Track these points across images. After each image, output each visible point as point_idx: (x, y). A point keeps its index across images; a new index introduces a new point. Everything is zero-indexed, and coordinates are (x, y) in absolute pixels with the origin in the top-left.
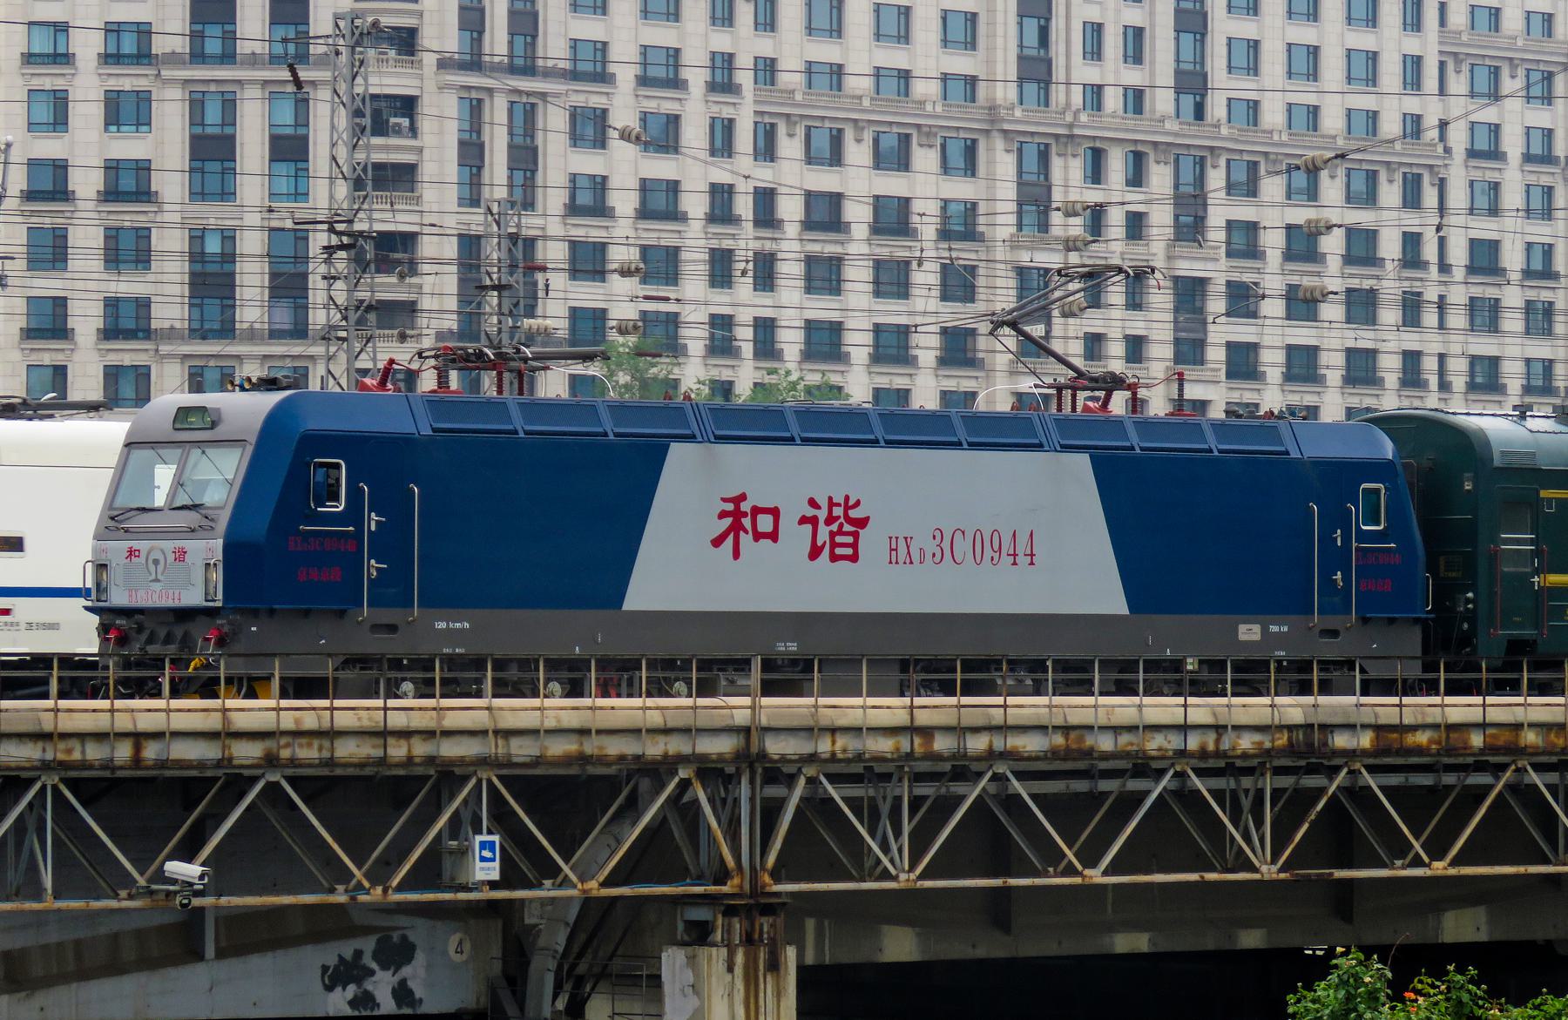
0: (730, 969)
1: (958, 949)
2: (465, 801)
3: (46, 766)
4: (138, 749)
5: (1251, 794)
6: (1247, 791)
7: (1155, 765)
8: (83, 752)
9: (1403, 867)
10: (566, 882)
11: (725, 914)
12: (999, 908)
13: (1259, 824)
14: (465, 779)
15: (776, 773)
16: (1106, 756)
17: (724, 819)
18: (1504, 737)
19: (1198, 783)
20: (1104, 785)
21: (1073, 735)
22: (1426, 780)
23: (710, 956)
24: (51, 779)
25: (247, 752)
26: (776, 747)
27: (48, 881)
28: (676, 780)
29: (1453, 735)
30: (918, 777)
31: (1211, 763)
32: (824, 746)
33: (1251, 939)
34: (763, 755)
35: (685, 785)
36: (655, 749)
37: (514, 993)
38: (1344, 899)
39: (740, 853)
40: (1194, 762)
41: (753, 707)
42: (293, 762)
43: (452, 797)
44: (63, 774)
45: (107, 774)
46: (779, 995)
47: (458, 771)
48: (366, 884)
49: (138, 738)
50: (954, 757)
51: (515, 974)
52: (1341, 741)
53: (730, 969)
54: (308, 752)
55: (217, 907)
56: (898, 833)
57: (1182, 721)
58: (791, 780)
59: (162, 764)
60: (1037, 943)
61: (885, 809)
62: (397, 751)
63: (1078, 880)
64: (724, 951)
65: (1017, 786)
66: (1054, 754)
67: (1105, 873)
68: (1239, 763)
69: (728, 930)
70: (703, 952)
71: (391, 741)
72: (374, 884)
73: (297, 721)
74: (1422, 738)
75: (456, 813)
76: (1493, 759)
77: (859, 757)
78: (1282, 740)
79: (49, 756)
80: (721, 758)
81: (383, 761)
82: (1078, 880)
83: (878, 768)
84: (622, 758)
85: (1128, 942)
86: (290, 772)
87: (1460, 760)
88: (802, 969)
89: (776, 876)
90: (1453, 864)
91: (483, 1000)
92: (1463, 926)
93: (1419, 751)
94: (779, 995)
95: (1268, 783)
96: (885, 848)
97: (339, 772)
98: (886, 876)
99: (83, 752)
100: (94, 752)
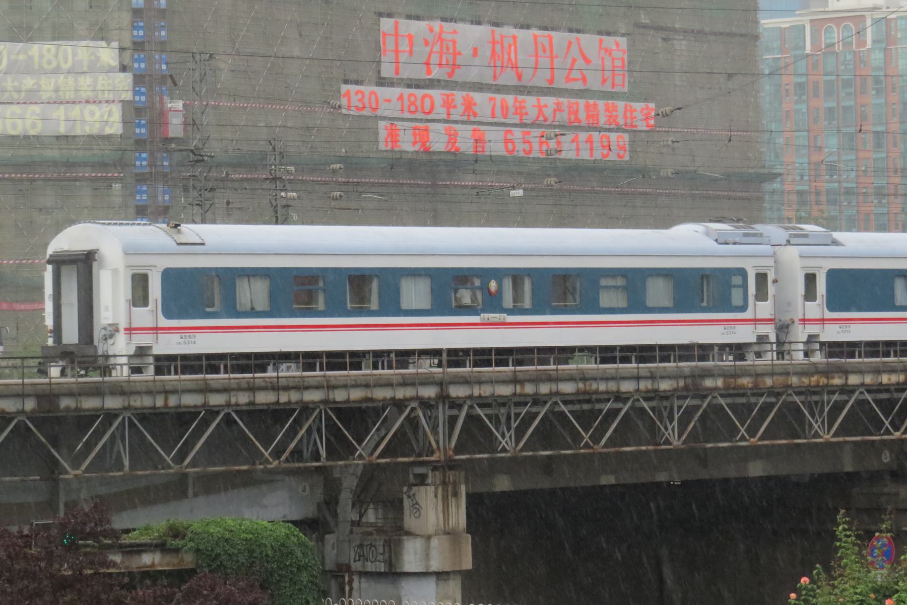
0: (436, 496)
1: (526, 484)
2: (314, 421)
3: (125, 409)
4: (166, 399)
5: (668, 409)
6: (665, 408)
7: (623, 396)
8: (142, 401)
9: (737, 441)
10: (360, 456)
11: (433, 470)
12: (548, 466)
13: (671, 421)
14: (314, 409)
15: (456, 404)
16: (602, 393)
17: (431, 426)
18: (780, 380)
19: (645, 405)
20: (598, 406)
21: (588, 383)
22: (743, 400)
23: (426, 491)
24: (127, 414)
25: (216, 400)
26: (457, 392)
27: (127, 463)
28: (409, 408)
29: (760, 379)
30: (517, 404)
31: (650, 395)
32: (476, 393)
33: (662, 477)
34: (448, 396)
35: (413, 409)
36: (401, 393)
37: (329, 510)
38: (703, 458)
39: (442, 442)
40: (643, 395)
41: (443, 373)
42: (237, 405)
43: (307, 419)
44: (134, 412)
45: (152, 411)
46: (458, 507)
47: (311, 406)
48: (271, 460)
49: (167, 393)
50: (536, 394)
51: (331, 502)
52: (709, 383)
53: (436, 496)
54: (243, 398)
55: (194, 473)
56: (509, 429)
57: (636, 374)
58: (460, 407)
59: (179, 406)
60: (566, 479)
61: (503, 419)
62: (284, 398)
63: (591, 451)
64: (433, 488)
65: (563, 408)
66: (578, 393)
67: (605, 446)
68: (662, 394)
69: (434, 477)
70: (422, 488)
71: (281, 392)
72: (274, 460)
73: (238, 383)
74: (746, 381)
75: (310, 426)
76: (776, 390)
77: (493, 395)
78: (681, 383)
79: (126, 404)
80: (429, 398)
81: (278, 403)
82: (591, 451)
83: (500, 400)
84: (385, 399)
85: (608, 480)
86: (234, 408)
87: (763, 391)
88: (467, 494)
89: (457, 451)
90: (759, 440)
91: (316, 513)
92: (756, 469)
93: (742, 387)
94: (458, 507)
95: (676, 403)
96: (503, 436)
97: (258, 407)
98: (504, 450)
99: (142, 401)
100: (147, 401)
